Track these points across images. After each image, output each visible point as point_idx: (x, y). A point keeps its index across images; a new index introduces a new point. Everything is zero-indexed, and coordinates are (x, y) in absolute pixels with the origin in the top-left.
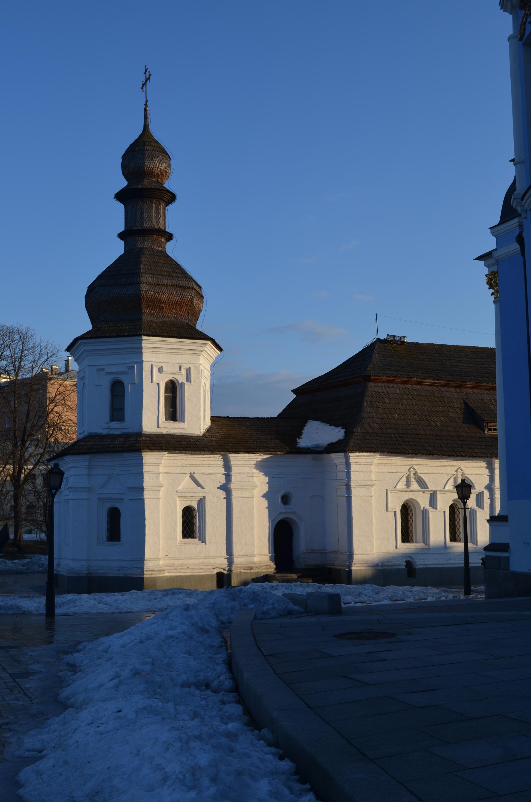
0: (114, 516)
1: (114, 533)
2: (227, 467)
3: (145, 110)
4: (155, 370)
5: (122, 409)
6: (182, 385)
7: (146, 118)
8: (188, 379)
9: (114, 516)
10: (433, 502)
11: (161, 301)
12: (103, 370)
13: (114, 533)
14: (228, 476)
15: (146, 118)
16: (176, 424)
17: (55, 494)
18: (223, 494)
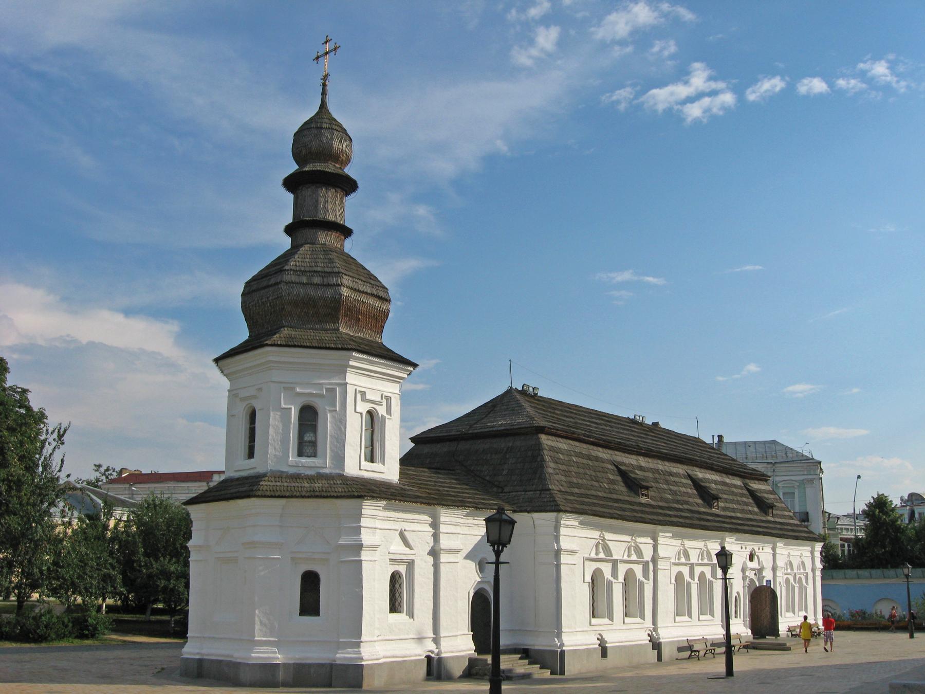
0: (310, 582)
1: (310, 604)
2: (435, 525)
3: (324, 85)
4: (359, 396)
5: (314, 444)
6: (383, 418)
7: (324, 93)
8: (389, 411)
9: (310, 582)
10: (615, 573)
11: (358, 312)
12: (293, 389)
13: (310, 604)
14: (436, 537)
15: (324, 93)
16: (377, 466)
17: (502, 550)
18: (431, 560)
